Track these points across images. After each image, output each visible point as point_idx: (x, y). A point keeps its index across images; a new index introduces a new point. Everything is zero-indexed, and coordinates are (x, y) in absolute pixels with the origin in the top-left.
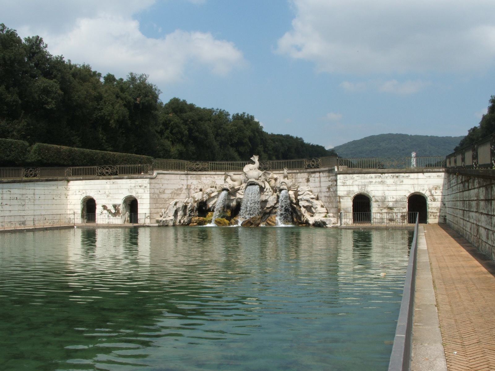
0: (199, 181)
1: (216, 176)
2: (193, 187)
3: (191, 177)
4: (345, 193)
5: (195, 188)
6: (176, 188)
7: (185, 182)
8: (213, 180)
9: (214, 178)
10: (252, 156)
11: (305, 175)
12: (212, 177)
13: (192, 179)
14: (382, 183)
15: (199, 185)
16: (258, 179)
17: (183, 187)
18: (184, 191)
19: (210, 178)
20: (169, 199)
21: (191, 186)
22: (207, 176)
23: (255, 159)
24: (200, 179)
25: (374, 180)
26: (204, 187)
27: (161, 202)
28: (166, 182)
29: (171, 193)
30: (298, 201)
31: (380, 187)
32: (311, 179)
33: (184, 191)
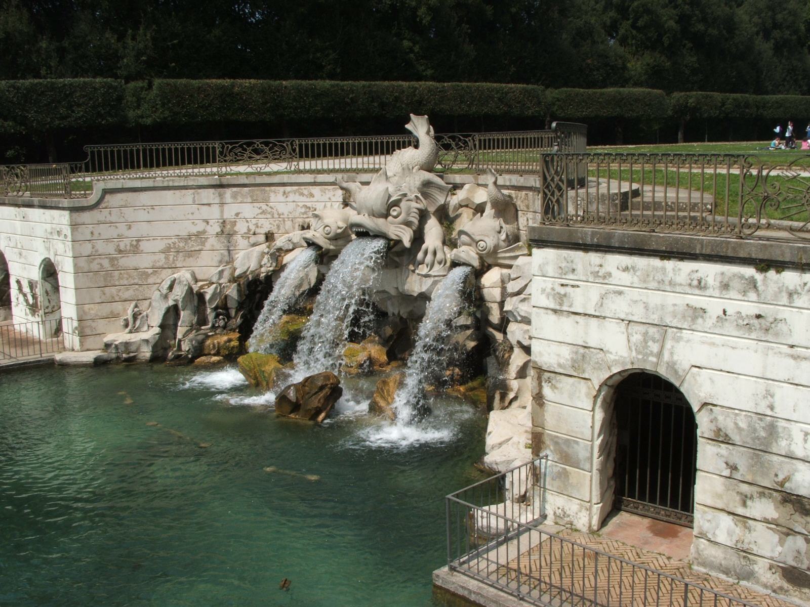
0: (264, 207)
1: (316, 190)
2: (241, 227)
3: (234, 196)
4: (566, 353)
5: (249, 230)
6: (184, 233)
7: (214, 213)
8: (309, 204)
9: (312, 195)
10: (408, 120)
12: (306, 192)
13: (240, 199)
14: (761, 326)
15: (261, 222)
16: (386, 215)
17: (208, 228)
18: (212, 242)
19: (297, 197)
20: (157, 269)
21: (234, 223)
22: (288, 189)
23: (419, 127)
24: (266, 201)
25: (714, 305)
26: (278, 227)
27: (126, 282)
28: (142, 215)
29: (166, 251)
31: (747, 355)
33: (212, 242)
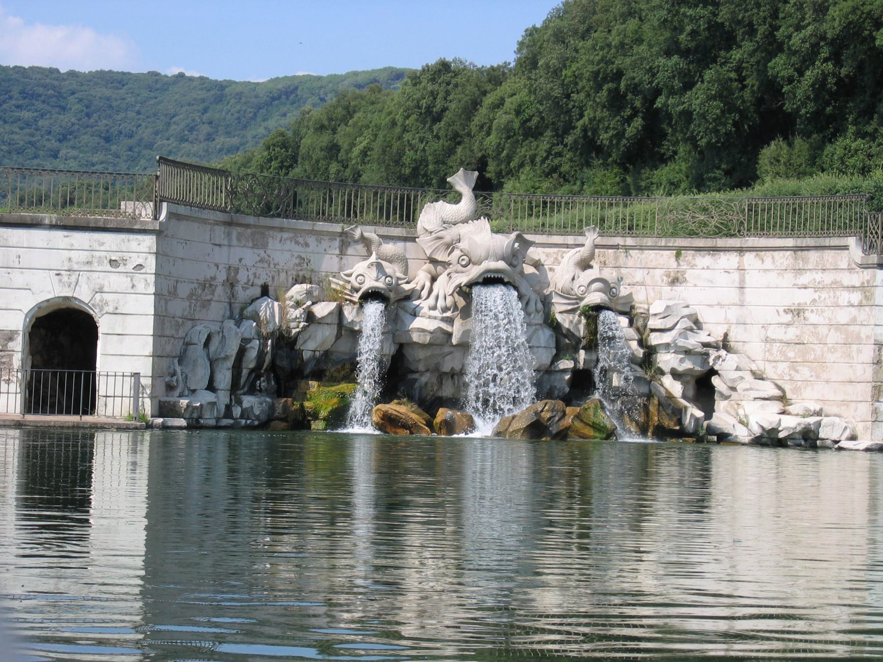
0: (262, 252)
2: (242, 277)
5: (249, 280)
8: (303, 256)
9: (307, 245)
11: (667, 258)
12: (301, 240)
15: (259, 271)
18: (220, 290)
19: (289, 245)
21: (237, 271)
24: (265, 246)
26: (273, 278)
30: (650, 352)
32: (690, 274)
33: (220, 290)
